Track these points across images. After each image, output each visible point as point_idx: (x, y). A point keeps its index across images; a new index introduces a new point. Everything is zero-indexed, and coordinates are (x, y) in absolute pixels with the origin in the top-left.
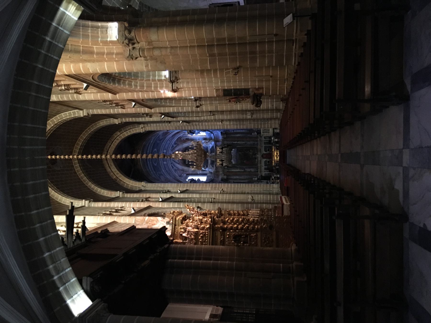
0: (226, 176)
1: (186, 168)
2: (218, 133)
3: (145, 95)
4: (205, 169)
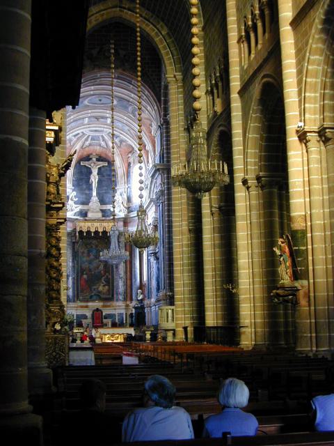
3: (291, 80)
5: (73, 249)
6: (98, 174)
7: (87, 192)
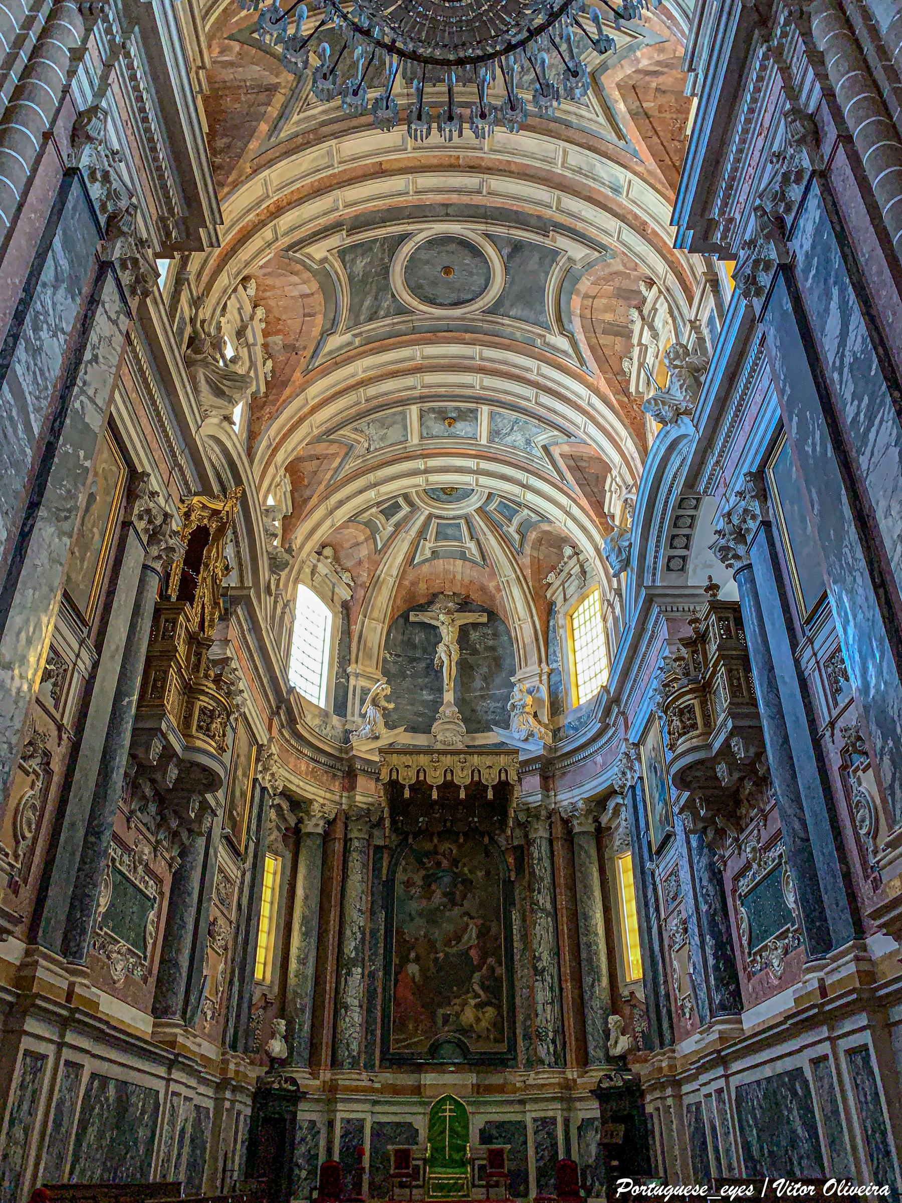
0: (320, 830)
2: (605, 767)
4: (375, 703)
5: (377, 870)
6: (459, 641)
7: (427, 696)
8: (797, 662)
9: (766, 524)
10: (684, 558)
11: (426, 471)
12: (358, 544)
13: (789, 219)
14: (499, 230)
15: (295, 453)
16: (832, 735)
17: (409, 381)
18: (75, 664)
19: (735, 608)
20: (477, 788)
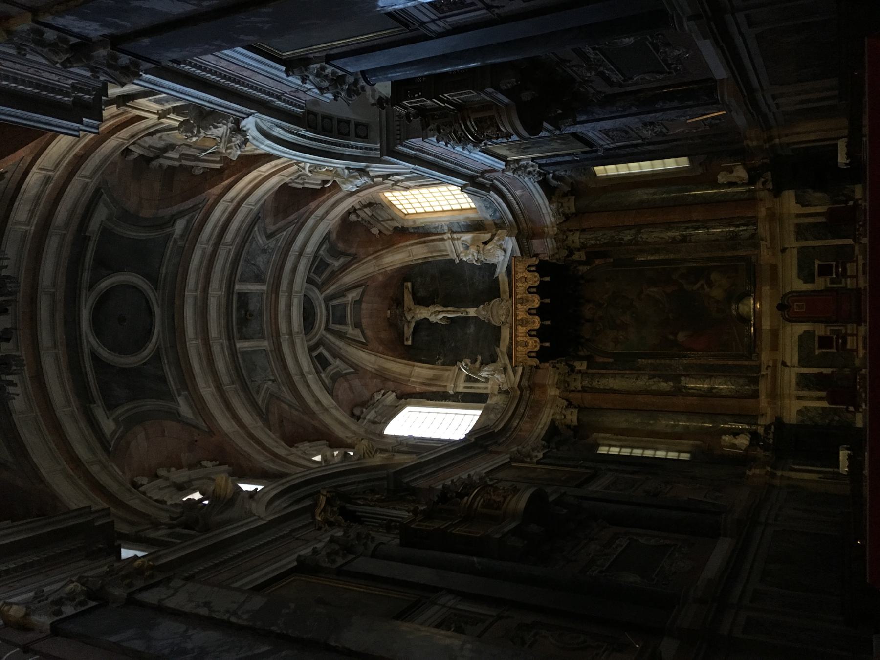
0: (576, 411)
1: (396, 367)
2: (524, 188)
5: (605, 366)
6: (428, 306)
7: (471, 330)
8: (440, 35)
9: (329, 59)
10: (357, 124)
11: (290, 334)
12: (351, 388)
13: (74, 40)
14: (86, 276)
15: (278, 440)
16: (497, 7)
17: (216, 348)
18: (450, 608)
19: (396, 85)
20: (541, 290)
